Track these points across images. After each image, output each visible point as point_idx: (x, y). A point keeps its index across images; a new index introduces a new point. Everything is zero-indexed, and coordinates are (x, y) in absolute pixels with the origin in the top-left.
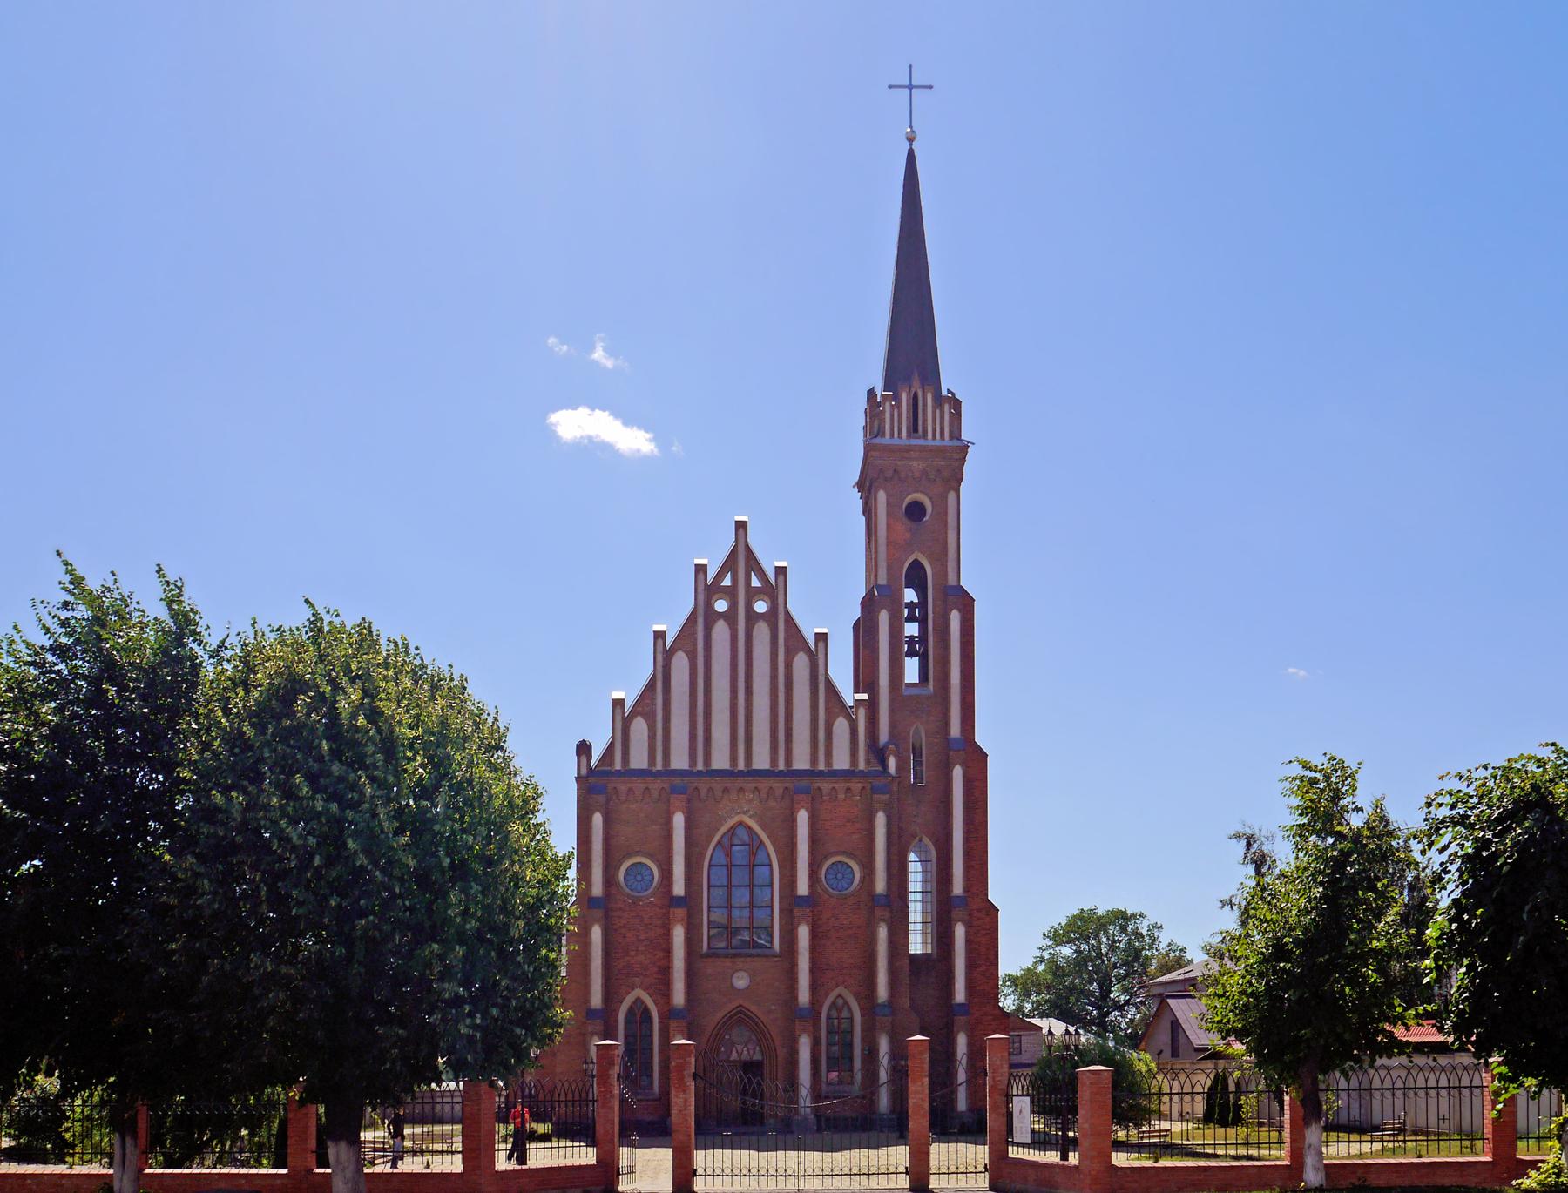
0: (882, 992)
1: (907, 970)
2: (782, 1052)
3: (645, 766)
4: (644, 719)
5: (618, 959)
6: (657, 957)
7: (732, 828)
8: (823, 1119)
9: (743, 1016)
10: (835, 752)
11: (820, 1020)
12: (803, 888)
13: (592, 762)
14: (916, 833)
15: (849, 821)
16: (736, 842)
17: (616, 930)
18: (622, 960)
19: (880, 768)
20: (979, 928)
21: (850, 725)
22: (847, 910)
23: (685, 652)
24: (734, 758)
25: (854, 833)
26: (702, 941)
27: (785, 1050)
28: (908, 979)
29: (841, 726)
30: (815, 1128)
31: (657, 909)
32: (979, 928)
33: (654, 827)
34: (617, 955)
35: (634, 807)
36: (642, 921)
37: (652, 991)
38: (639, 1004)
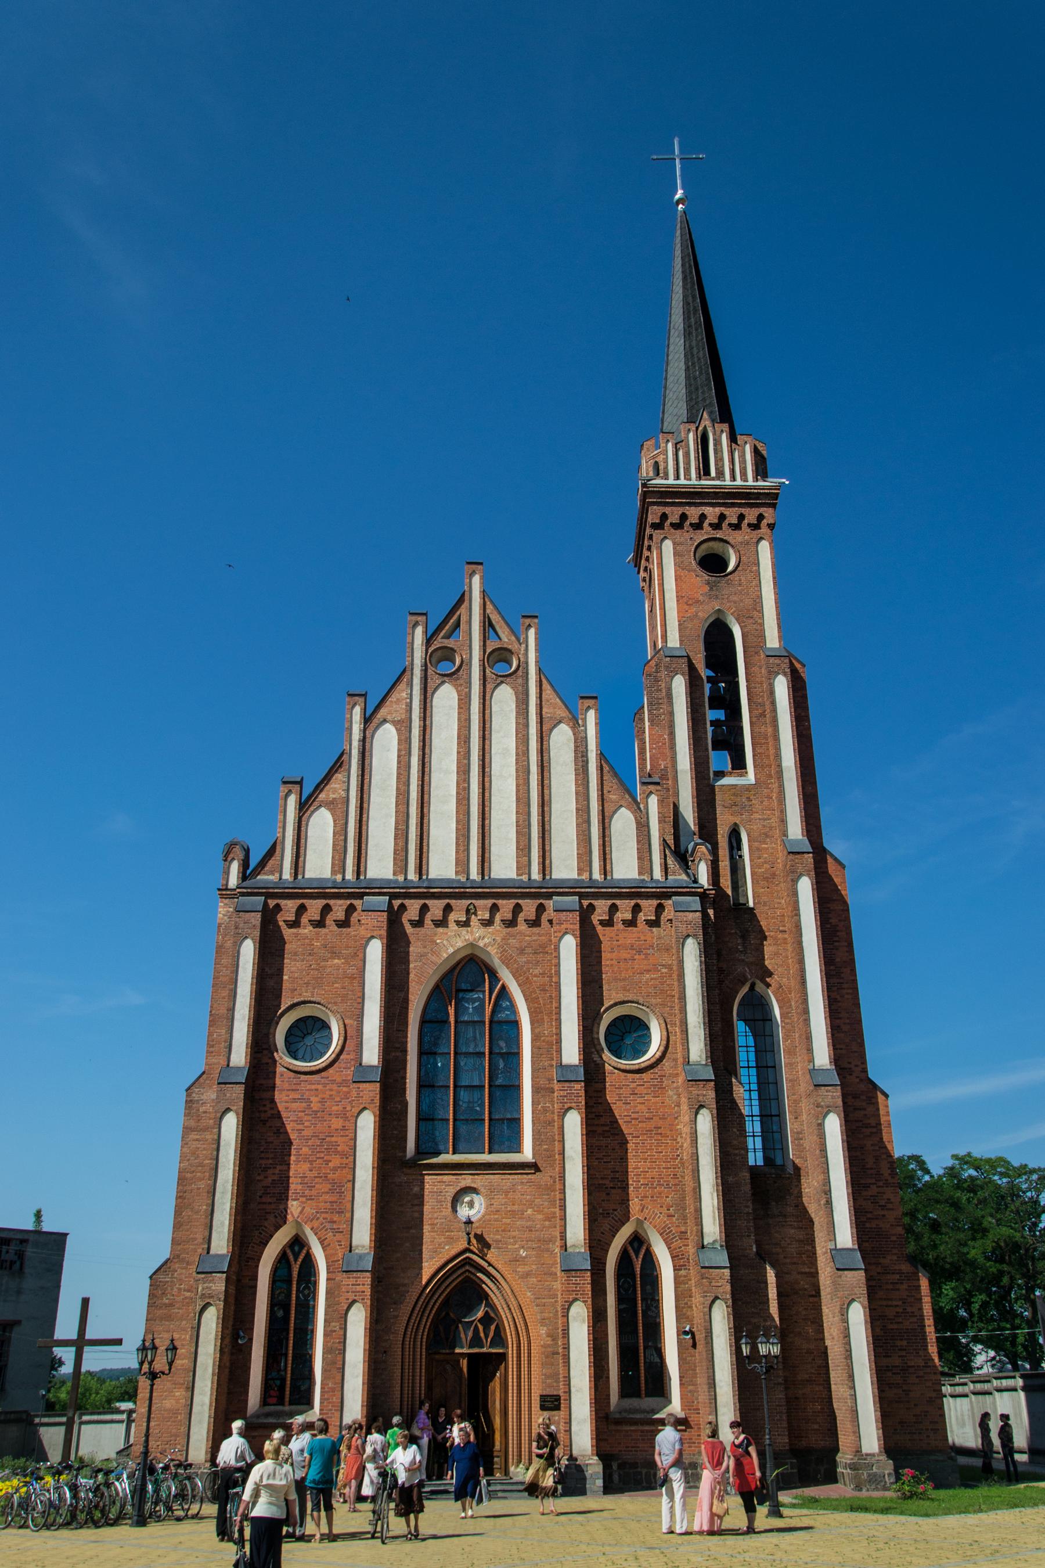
0: (712, 1228)
1: (747, 1188)
2: (539, 1334)
3: (326, 872)
4: (330, 810)
5: (265, 1169)
6: (330, 1164)
7: (458, 963)
8: (615, 1466)
9: (472, 1269)
10: (615, 855)
11: (604, 1277)
12: (571, 1053)
13: (248, 872)
14: (744, 976)
15: (639, 952)
16: (463, 986)
17: (264, 1122)
18: (270, 1172)
19: (684, 877)
20: (860, 1124)
21: (636, 818)
22: (640, 1090)
23: (394, 723)
24: (462, 863)
25: (648, 971)
26: (404, 1139)
27: (543, 1331)
28: (750, 1204)
29: (623, 822)
30: (600, 1482)
31: (335, 1087)
32: (860, 1124)
33: (336, 961)
34: (263, 1162)
35: (306, 931)
36: (309, 1107)
37: (316, 1224)
38: (296, 1248)
